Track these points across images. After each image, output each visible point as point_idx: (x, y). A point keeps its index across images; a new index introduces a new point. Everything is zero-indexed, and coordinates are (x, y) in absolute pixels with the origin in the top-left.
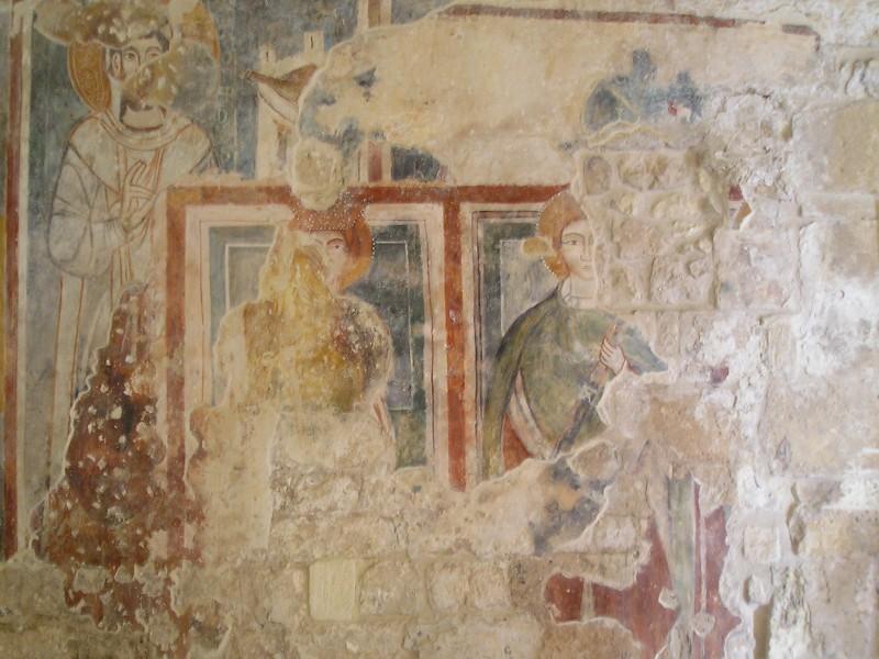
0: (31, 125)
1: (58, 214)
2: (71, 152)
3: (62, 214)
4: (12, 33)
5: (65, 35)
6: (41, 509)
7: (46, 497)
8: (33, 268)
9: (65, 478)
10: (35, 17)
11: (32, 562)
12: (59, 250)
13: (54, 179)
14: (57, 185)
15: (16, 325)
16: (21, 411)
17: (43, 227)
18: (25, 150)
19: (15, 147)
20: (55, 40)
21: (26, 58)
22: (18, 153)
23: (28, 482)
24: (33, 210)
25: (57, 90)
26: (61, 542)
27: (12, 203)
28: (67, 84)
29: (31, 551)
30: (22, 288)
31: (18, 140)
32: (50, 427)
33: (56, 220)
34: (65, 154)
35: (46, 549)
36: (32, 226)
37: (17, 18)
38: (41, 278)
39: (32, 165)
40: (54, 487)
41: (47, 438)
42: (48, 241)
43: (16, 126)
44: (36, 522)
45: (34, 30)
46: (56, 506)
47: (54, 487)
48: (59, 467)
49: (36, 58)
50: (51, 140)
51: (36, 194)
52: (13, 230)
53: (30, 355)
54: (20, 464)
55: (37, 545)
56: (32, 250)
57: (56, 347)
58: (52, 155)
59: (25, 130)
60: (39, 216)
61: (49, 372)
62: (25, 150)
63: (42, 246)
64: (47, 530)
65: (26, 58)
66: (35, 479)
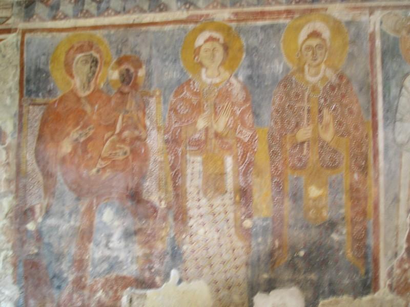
0: (383, 75)
1: (398, 121)
2: (403, 90)
3: (401, 120)
4: (371, 30)
5: (398, 32)
6: (392, 268)
7: (395, 262)
8: (387, 148)
9: (405, 253)
10: (381, 23)
11: (387, 295)
12: (401, 138)
13: (396, 103)
14: (397, 107)
15: (378, 176)
16: (382, 218)
17: (391, 127)
18: (380, 89)
19: (375, 88)
20: (392, 35)
21: (378, 43)
22: (376, 90)
23: (386, 255)
24: (386, 118)
25: (395, 59)
26: (402, 286)
27: (374, 115)
28: (399, 56)
29: (387, 290)
30: (381, 157)
31: (376, 83)
32: (397, 228)
33: (398, 124)
34: (401, 91)
35: (395, 289)
36: (385, 126)
37: (372, 23)
38: (391, 153)
39: (384, 97)
40: (399, 257)
41: (395, 233)
42: (394, 134)
43: (374, 76)
44: (390, 274)
45: (381, 30)
46: (400, 266)
47: (399, 257)
48: (401, 247)
49: (383, 43)
50: (393, 83)
51: (387, 110)
52: (375, 128)
53: (387, 191)
54: (382, 246)
55: (390, 286)
56: (386, 138)
57: (400, 186)
58: (394, 91)
59: (380, 78)
60: (389, 122)
61: (396, 199)
62: (380, 89)
63: (391, 136)
64: (395, 279)
65: (378, 43)
66: (390, 253)
